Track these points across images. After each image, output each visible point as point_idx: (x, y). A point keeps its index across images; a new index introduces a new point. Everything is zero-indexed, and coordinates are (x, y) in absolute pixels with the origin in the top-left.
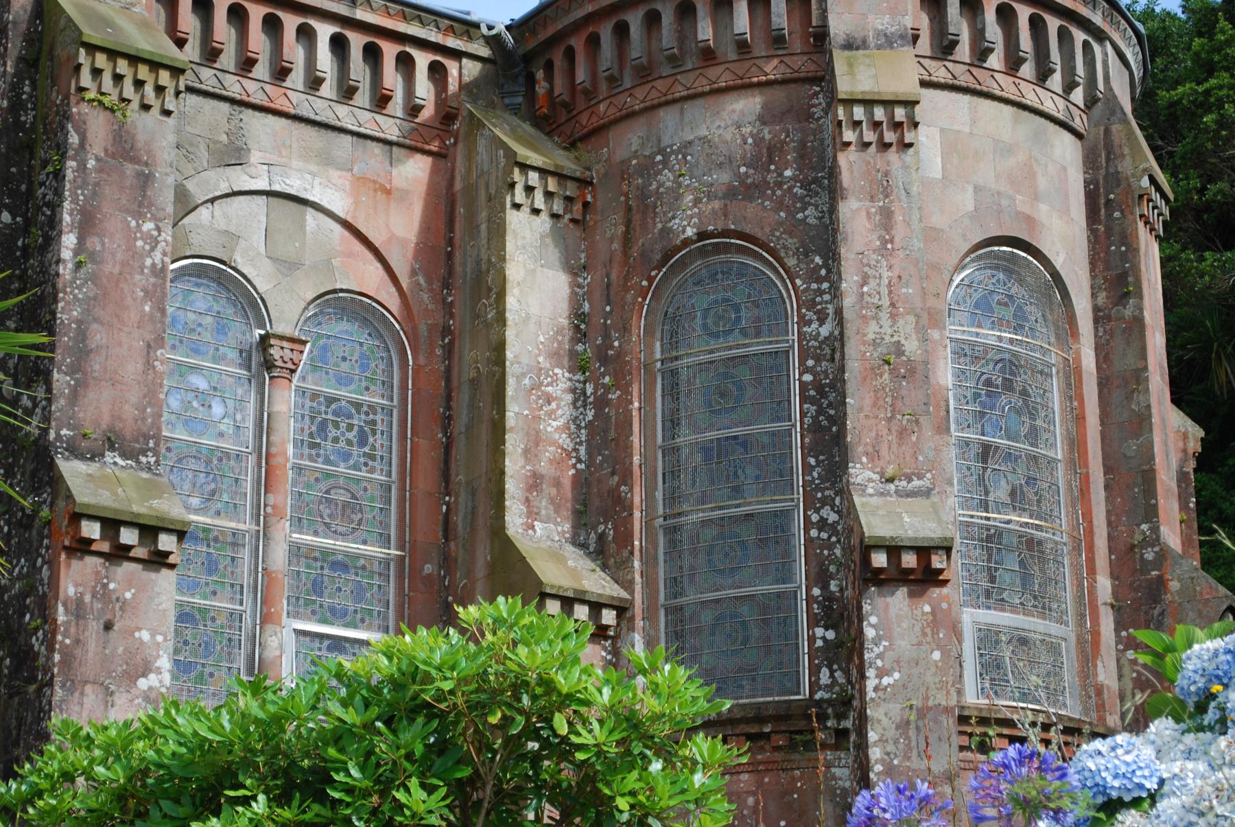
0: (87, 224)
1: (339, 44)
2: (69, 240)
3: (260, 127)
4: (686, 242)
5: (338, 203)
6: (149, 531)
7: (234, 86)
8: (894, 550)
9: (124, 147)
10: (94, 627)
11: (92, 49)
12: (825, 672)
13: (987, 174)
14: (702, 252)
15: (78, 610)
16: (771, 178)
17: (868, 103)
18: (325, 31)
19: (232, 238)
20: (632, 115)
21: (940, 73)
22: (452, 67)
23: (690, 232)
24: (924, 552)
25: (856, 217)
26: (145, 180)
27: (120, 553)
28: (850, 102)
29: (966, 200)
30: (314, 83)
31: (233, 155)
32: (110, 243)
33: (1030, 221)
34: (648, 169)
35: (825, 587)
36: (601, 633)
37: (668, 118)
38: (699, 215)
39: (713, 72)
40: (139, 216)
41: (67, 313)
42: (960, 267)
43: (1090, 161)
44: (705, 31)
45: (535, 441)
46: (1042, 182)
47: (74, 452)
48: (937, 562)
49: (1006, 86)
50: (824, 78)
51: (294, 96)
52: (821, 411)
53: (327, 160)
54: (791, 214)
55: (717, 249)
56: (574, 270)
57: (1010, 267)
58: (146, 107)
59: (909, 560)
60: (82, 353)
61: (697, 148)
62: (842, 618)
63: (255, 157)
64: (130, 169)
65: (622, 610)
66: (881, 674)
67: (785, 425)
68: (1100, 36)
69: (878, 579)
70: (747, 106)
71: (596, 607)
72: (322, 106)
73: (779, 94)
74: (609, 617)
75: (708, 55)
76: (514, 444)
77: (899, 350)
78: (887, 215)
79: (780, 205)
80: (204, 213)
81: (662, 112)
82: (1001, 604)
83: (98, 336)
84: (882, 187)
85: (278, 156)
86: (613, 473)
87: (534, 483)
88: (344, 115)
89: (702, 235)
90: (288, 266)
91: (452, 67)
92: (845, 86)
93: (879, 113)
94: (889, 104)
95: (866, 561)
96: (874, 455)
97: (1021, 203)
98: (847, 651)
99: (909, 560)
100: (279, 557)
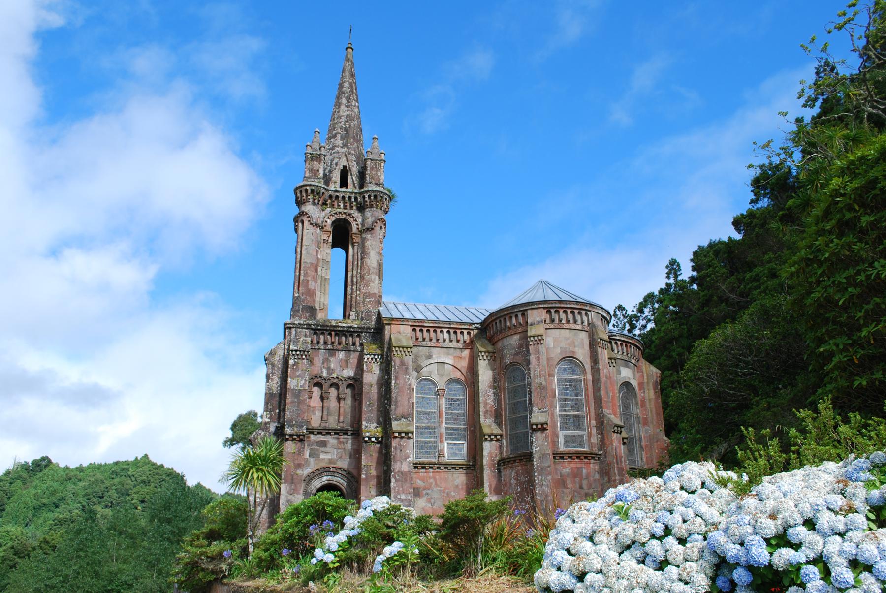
0: (396, 378)
1: (449, 332)
2: (393, 382)
3: (435, 351)
5: (451, 362)
6: (407, 433)
7: (429, 344)
8: (537, 425)
9: (403, 363)
10: (398, 451)
13: (563, 345)
15: (396, 448)
17: (534, 337)
18: (445, 330)
19: (430, 372)
21: (552, 326)
22: (472, 332)
24: (542, 424)
25: (533, 358)
26: (407, 369)
27: (402, 438)
29: (558, 351)
30: (444, 340)
31: (430, 357)
32: (401, 382)
33: (573, 352)
34: (502, 350)
36: (498, 440)
37: (505, 340)
41: (393, 395)
42: (558, 364)
43: (590, 336)
44: (508, 324)
45: (486, 404)
46: (576, 343)
47: (396, 419)
48: (545, 426)
49: (567, 326)
51: (441, 343)
53: (448, 354)
56: (493, 369)
57: (571, 362)
59: (540, 426)
60: (396, 402)
65: (501, 435)
68: (590, 311)
69: (534, 430)
70: (517, 337)
71: (496, 436)
72: (446, 344)
74: (499, 437)
75: (510, 328)
76: (482, 405)
78: (539, 357)
82: (569, 429)
83: (399, 398)
84: (537, 352)
85: (438, 356)
87: (486, 412)
88: (451, 345)
90: (441, 375)
91: (472, 332)
94: (538, 336)
96: (537, 405)
97: (571, 349)
99: (540, 426)
100: (443, 430)
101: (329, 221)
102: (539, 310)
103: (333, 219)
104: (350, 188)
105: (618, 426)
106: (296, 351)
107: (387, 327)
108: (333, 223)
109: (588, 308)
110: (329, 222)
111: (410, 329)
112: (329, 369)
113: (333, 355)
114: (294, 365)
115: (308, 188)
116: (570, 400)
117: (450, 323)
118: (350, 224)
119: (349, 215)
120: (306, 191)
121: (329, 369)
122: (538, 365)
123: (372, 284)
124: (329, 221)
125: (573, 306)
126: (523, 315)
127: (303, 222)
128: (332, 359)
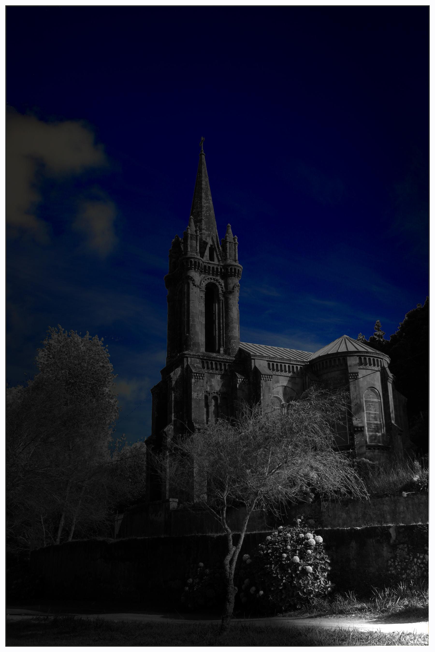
2: (262, 397)
3: (280, 377)
7: (277, 373)
11: (263, 375)
18: (287, 365)
26: (269, 389)
28: (350, 374)
29: (366, 383)
33: (374, 384)
40: (269, 393)
46: (375, 379)
50: (347, 369)
57: (372, 390)
58: (268, 380)
59: (359, 429)
62: (352, 435)
63: (280, 382)
64: (268, 388)
69: (355, 431)
77: (357, 403)
78: (355, 387)
80: (275, 389)
92: (349, 371)
93: (354, 375)
95: (354, 429)
98: (353, 439)
101: (204, 283)
102: (354, 357)
103: (206, 282)
104: (216, 262)
105: (401, 431)
106: (196, 373)
107: (253, 361)
108: (206, 285)
109: (381, 357)
110: (204, 284)
111: (266, 363)
112: (211, 386)
113: (213, 377)
114: (195, 383)
115: (192, 260)
116: (372, 414)
117: (290, 360)
118: (217, 286)
119: (217, 280)
120: (191, 261)
121: (211, 386)
122: (355, 391)
123: (235, 330)
124: (204, 283)
125: (374, 355)
127: (189, 284)
128: (213, 380)
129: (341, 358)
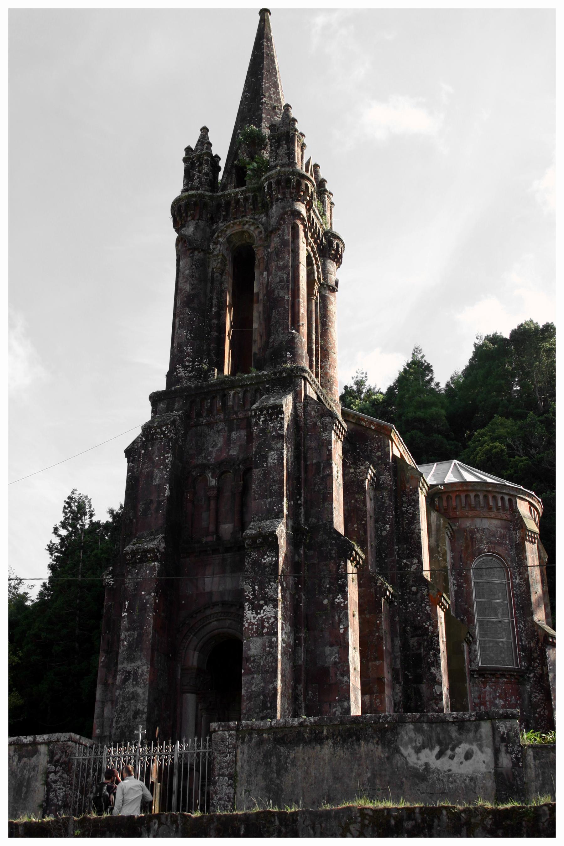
4: (485, 552)
12: (523, 663)
14: (486, 556)
16: (504, 542)
20: (467, 517)
23: (486, 550)
35: (522, 642)
38: (488, 547)
39: (490, 513)
52: (518, 601)
54: (509, 552)
55: (490, 556)
61: (486, 530)
66: (550, 666)
67: (477, 600)
70: (495, 522)
73: (503, 522)
79: (506, 550)
81: (476, 519)
86: (466, 604)
89: (489, 552)
126: (510, 500)
129: (506, 498)
